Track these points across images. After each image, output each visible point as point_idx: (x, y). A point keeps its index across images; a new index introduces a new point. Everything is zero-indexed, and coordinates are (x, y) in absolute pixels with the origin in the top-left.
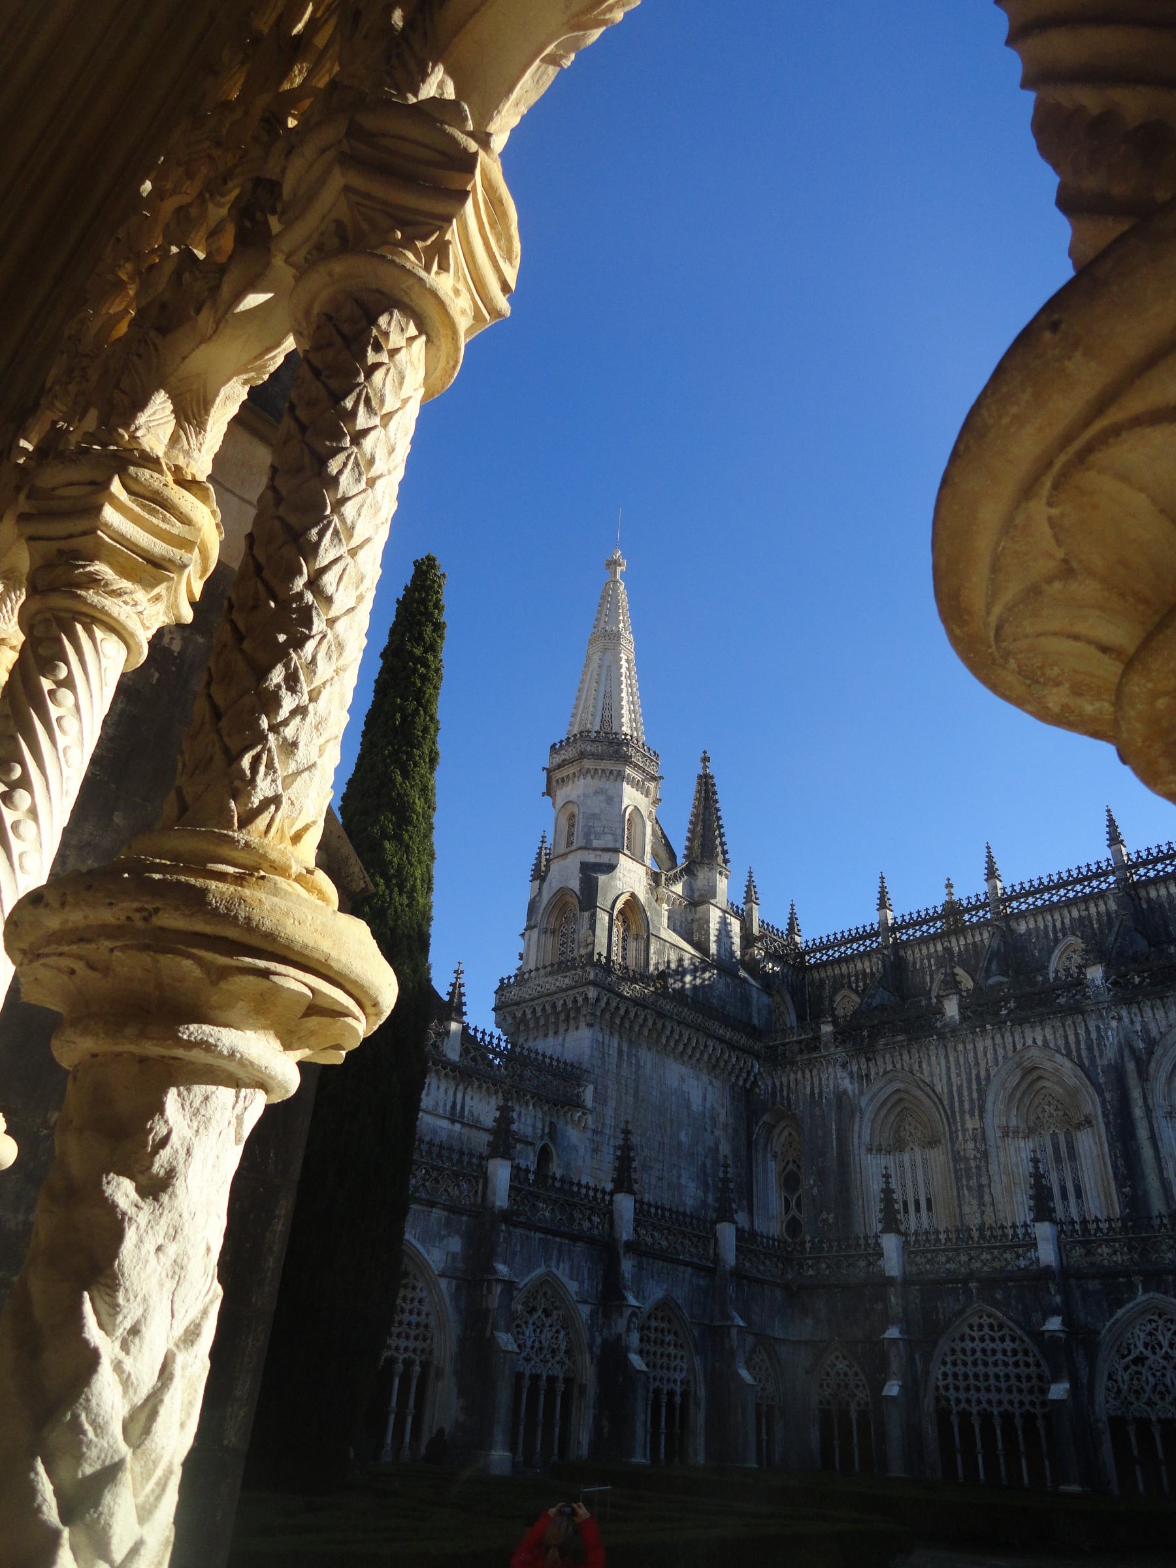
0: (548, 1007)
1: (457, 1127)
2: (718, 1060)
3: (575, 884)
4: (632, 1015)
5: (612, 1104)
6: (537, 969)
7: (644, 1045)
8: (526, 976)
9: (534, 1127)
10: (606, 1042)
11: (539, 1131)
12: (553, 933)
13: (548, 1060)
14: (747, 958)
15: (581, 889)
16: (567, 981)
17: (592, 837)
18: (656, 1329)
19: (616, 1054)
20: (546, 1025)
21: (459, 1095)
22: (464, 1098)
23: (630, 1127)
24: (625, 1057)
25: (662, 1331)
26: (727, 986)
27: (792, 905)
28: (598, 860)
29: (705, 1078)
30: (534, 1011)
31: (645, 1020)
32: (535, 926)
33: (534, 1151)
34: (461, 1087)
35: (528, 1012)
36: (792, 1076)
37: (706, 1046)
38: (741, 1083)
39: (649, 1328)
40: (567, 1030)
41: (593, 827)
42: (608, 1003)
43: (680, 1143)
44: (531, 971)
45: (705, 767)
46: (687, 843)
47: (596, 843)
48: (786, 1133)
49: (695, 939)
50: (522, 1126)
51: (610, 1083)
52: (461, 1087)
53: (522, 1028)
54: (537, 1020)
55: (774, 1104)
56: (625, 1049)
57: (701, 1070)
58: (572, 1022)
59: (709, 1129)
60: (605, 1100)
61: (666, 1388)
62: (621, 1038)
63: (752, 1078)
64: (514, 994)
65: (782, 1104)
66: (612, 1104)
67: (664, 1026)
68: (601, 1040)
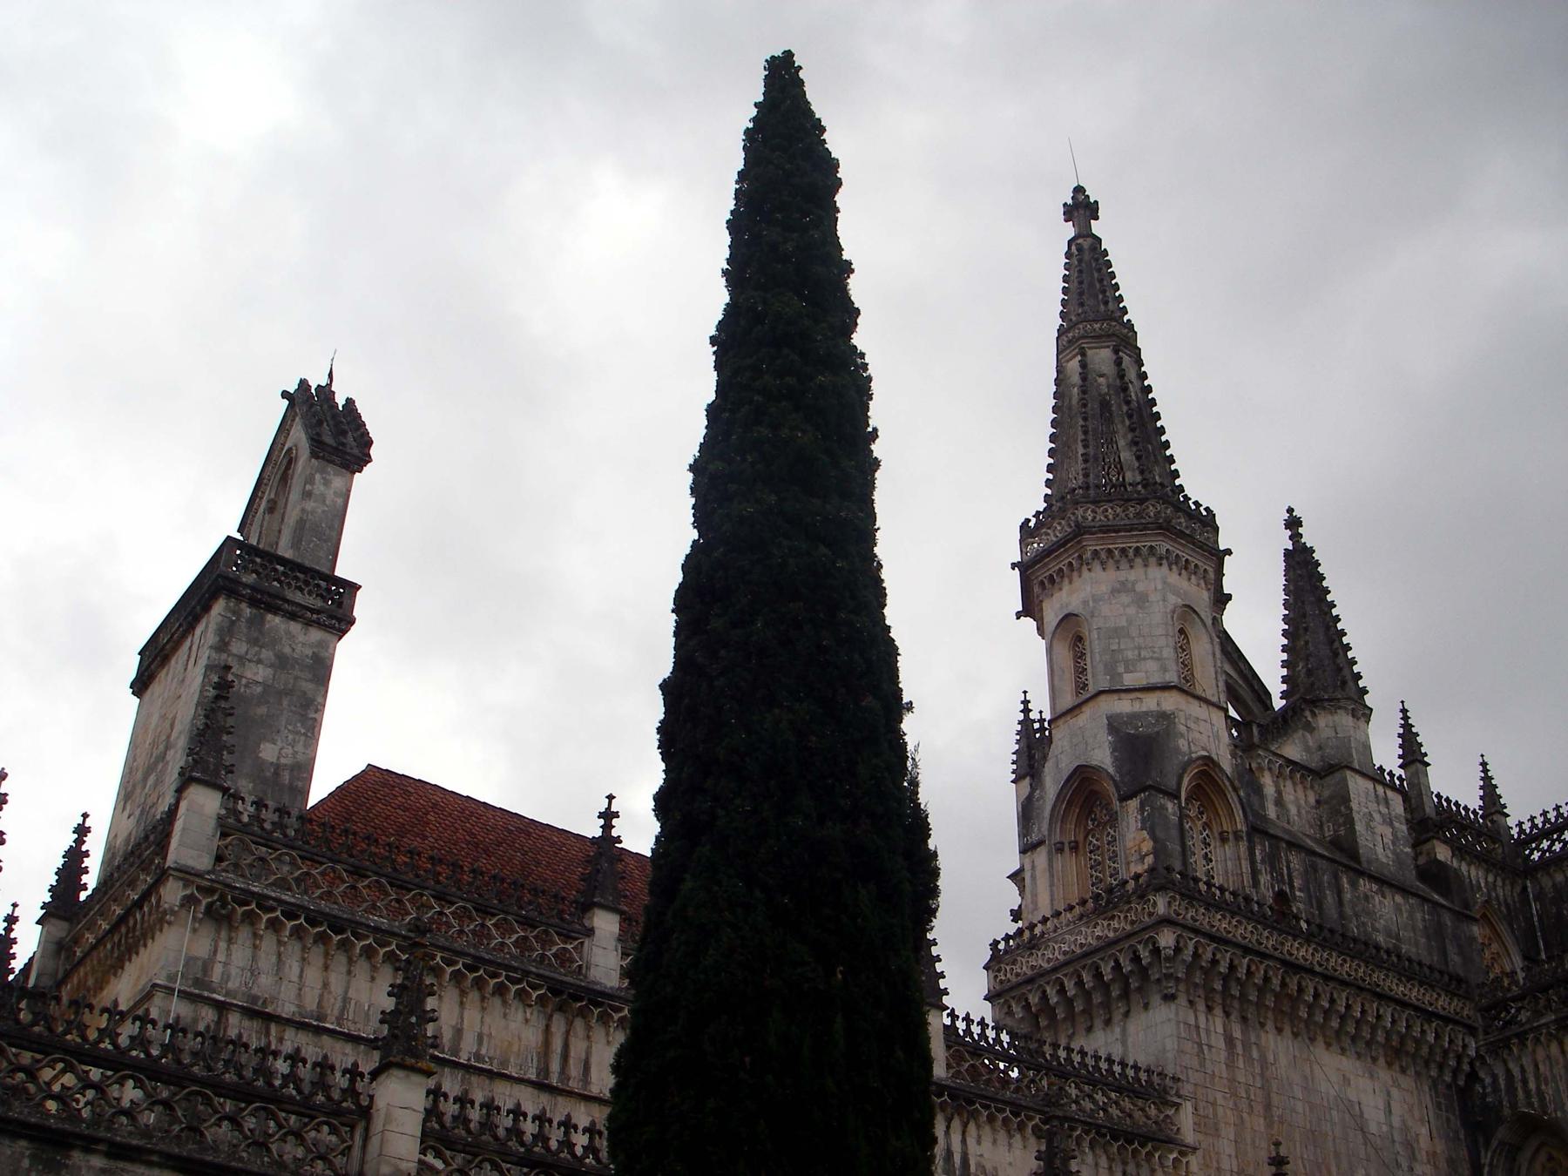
0: (1086, 977)
2: (1402, 1038)
3: (1102, 756)
4: (1242, 973)
6: (1057, 914)
7: (1270, 1025)
8: (1037, 931)
10: (1202, 1025)
12: (1075, 848)
13: (1104, 1066)
14: (1422, 860)
15: (1116, 759)
16: (1115, 924)
17: (1121, 669)
19: (1222, 1044)
20: (1087, 1012)
21: (956, 1139)
22: (964, 1141)
23: (1283, 1152)
24: (1239, 1049)
26: (1398, 908)
27: (1484, 764)
28: (1138, 707)
29: (1384, 1075)
30: (1062, 991)
31: (1266, 979)
32: (1040, 843)
34: (956, 1124)
35: (1051, 992)
36: (1541, 1054)
37: (1379, 1017)
38: (1448, 1078)
40: (1127, 1014)
41: (1120, 651)
42: (1196, 955)
44: (1045, 920)
45: (1296, 537)
46: (1284, 672)
47: (1129, 680)
48: (1542, 1157)
49: (1329, 833)
51: (1219, 1096)
52: (956, 1124)
53: (1043, 1022)
54: (1069, 1002)
55: (1514, 1106)
56: (1237, 1034)
57: (1374, 1060)
58: (1135, 997)
59: (1405, 1165)
62: (1227, 1014)
63: (1466, 1067)
64: (1025, 966)
65: (1530, 1105)
66: (1228, 1132)
67: (1301, 990)
68: (1192, 1022)
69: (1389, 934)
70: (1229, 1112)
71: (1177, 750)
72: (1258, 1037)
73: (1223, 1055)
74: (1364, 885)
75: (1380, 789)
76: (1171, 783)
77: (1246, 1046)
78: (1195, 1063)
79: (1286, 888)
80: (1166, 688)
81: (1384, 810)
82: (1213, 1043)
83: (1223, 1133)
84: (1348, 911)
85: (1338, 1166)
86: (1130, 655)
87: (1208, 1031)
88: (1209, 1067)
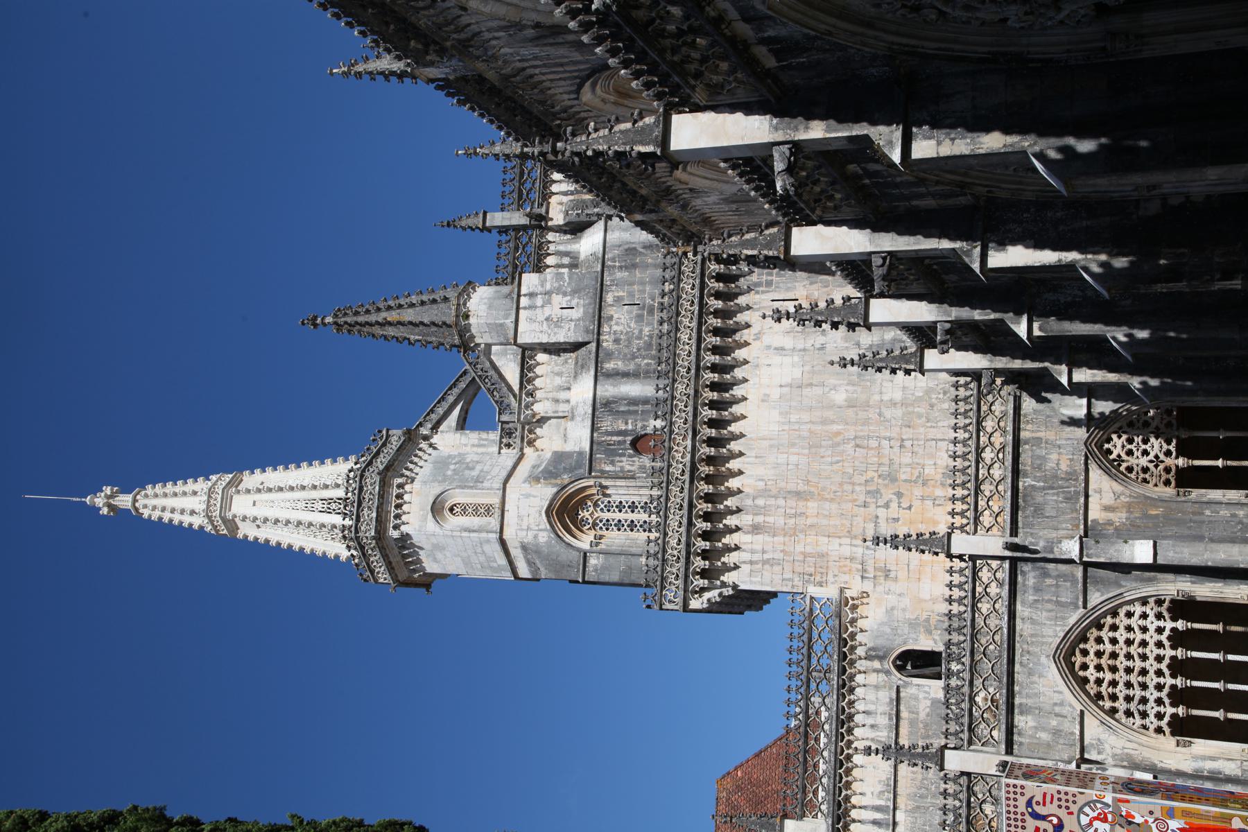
1: (900, 816)
5: (824, 544)
9: (877, 687)
11: (882, 677)
17: (495, 565)
18: (1099, 668)
19: (759, 538)
24: (760, 519)
25: (1099, 654)
33: (906, 684)
39: (1099, 682)
43: (851, 404)
47: (502, 561)
50: (881, 709)
51: (800, 548)
60: (822, 556)
61: (1168, 653)
66: (824, 544)
69: (639, 318)
70: (809, 539)
71: (548, 543)
72: (748, 495)
73: (768, 539)
74: (607, 344)
75: (524, 301)
76: (575, 557)
77: (757, 511)
78: (777, 569)
79: (629, 438)
80: (503, 543)
81: (539, 301)
82: (758, 547)
83: (824, 549)
84: (631, 367)
85: (833, 422)
86: (482, 558)
87: (753, 552)
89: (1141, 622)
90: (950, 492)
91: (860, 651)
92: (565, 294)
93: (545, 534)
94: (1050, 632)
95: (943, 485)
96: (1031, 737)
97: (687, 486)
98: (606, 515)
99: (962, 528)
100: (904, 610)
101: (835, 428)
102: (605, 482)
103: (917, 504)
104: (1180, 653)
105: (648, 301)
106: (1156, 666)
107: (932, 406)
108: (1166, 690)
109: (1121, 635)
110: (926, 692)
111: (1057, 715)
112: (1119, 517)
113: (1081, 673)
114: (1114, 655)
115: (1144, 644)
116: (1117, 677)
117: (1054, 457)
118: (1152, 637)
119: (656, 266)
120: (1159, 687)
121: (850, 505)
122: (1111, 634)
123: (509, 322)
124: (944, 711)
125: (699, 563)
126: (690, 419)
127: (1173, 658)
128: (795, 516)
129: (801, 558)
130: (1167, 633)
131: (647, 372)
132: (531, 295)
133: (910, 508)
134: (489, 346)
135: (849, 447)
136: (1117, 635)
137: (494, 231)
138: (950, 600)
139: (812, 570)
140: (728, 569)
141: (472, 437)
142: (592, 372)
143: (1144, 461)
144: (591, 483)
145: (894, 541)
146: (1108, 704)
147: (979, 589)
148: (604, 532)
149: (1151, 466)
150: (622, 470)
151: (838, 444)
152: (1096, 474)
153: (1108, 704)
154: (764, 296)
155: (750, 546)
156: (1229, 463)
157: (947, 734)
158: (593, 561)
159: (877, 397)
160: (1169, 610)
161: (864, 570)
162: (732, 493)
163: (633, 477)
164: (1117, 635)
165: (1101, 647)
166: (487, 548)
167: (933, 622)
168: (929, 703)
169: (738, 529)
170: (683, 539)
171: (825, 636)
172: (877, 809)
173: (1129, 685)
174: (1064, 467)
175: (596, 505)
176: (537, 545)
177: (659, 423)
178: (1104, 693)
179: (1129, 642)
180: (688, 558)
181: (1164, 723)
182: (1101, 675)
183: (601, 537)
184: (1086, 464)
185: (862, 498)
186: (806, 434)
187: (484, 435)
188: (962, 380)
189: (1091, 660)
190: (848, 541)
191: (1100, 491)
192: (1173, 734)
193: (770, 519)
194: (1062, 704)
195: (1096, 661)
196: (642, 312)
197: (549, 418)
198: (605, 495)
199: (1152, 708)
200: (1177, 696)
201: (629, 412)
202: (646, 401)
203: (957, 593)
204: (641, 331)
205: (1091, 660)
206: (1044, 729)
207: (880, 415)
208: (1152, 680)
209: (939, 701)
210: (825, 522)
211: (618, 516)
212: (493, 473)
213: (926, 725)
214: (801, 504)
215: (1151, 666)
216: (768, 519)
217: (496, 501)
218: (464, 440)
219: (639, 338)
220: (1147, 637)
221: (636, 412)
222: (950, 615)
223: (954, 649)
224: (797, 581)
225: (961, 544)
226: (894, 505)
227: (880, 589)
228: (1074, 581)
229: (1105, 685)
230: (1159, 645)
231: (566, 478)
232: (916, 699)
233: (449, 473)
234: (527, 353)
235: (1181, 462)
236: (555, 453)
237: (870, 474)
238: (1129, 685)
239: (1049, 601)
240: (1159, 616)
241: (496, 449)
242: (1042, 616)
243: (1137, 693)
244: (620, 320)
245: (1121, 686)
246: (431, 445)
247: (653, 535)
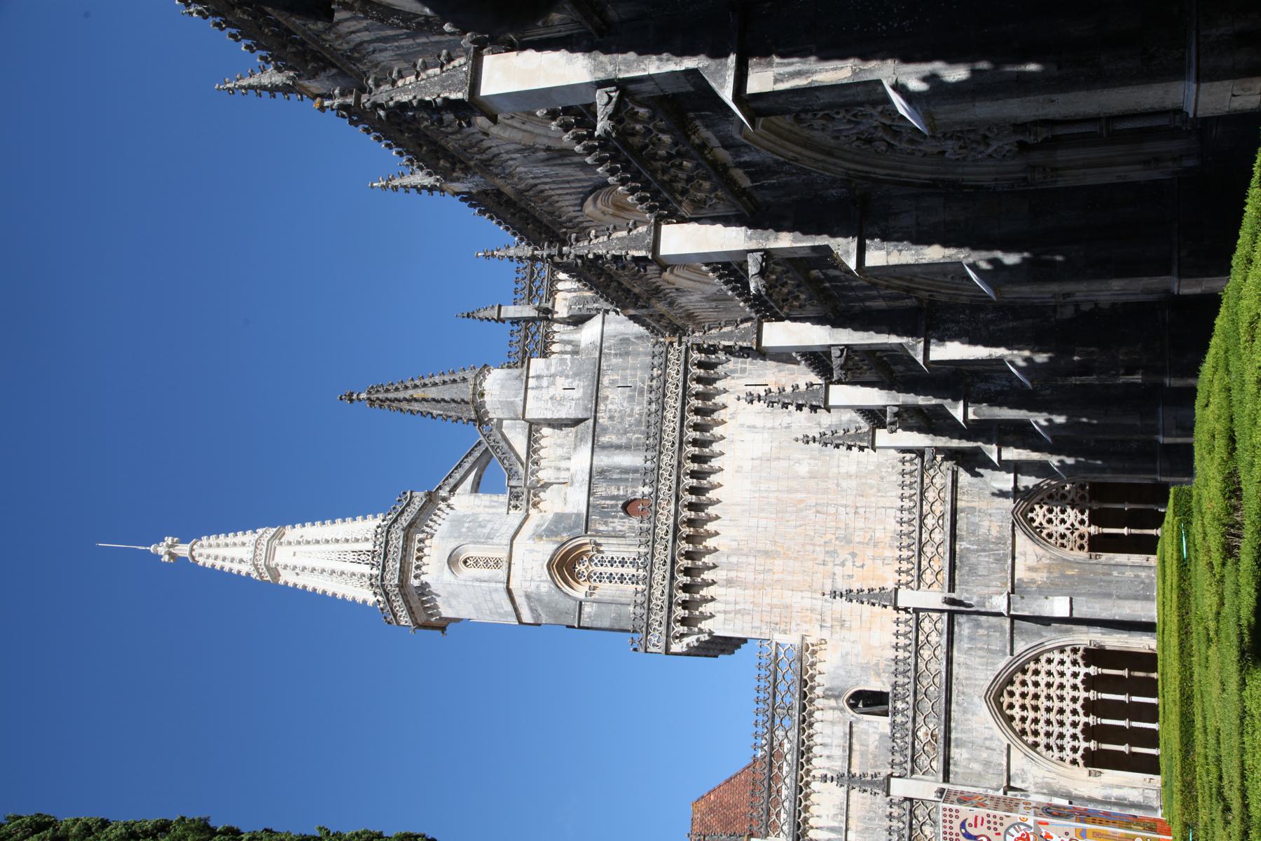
9: (833, 723)
11: (837, 713)
18: (1023, 707)
25: (1023, 695)
33: (858, 720)
39: (1023, 719)
43: (813, 476)
47: (509, 608)
50: (836, 742)
51: (767, 600)
61: (1082, 694)
69: (631, 398)
70: (775, 593)
72: (723, 554)
73: (740, 591)
74: (603, 420)
75: (532, 383)
76: (573, 605)
78: (747, 618)
79: (621, 503)
80: (509, 592)
81: (545, 382)
82: (732, 599)
84: (624, 441)
85: (797, 491)
86: (491, 605)
87: (726, 603)
88: (749, 607)
89: (1060, 668)
90: (898, 553)
91: (819, 691)
92: (567, 377)
93: (546, 585)
94: (982, 676)
95: (891, 547)
96: (965, 767)
97: (670, 544)
98: (599, 569)
99: (907, 584)
100: (857, 655)
101: (800, 496)
102: (599, 540)
103: (868, 563)
104: (1092, 695)
105: (639, 384)
106: (1072, 706)
107: (882, 478)
108: (1080, 727)
109: (1042, 679)
110: (875, 727)
111: (987, 748)
112: (1041, 577)
113: (1008, 712)
114: (1036, 697)
115: (1061, 686)
116: (1038, 715)
117: (986, 523)
118: (1068, 681)
119: (646, 354)
120: (1074, 725)
121: (811, 563)
122: (1034, 678)
123: (519, 400)
124: (890, 744)
125: (680, 612)
126: (674, 486)
127: (1086, 699)
128: (763, 572)
129: (768, 609)
130: (1081, 677)
131: (638, 445)
132: (538, 377)
133: (863, 566)
134: (500, 421)
135: (811, 514)
136: (1038, 678)
137: (508, 322)
138: (897, 648)
139: (777, 619)
140: (704, 617)
141: (484, 499)
142: (590, 445)
143: (1062, 529)
144: (587, 540)
145: (849, 595)
146: (1031, 739)
147: (921, 638)
148: (598, 584)
149: (1068, 533)
150: (614, 530)
151: (801, 510)
152: (1021, 538)
153: (1031, 739)
154: (738, 382)
155: (723, 598)
156: (1133, 531)
157: (892, 764)
158: (587, 609)
159: (835, 470)
160: (1083, 657)
161: (823, 620)
162: (709, 551)
163: (623, 537)
164: (1038, 678)
165: (1025, 689)
166: (495, 596)
167: (882, 666)
168: (877, 737)
169: (714, 583)
170: (666, 591)
171: (788, 677)
172: (832, 829)
173: (1048, 722)
174: (994, 532)
175: (591, 560)
176: (539, 594)
177: (647, 490)
178: (1028, 730)
179: (1049, 685)
180: (670, 608)
181: (1078, 756)
182: (1025, 714)
183: (595, 588)
184: (1013, 530)
185: (821, 557)
186: (773, 501)
187: (495, 498)
188: (908, 456)
189: (1017, 700)
190: (809, 594)
191: (1025, 554)
192: (1086, 765)
193: (742, 575)
194: (991, 739)
195: (1021, 701)
196: (634, 392)
197: (552, 484)
198: (599, 551)
199: (1068, 743)
200: (1090, 733)
201: (621, 480)
202: (636, 471)
203: (902, 641)
204: (632, 410)
205: (1017, 700)
206: (976, 760)
207: (837, 485)
208: (1068, 718)
209: (886, 735)
210: (789, 578)
211: (610, 570)
212: (502, 531)
213: (875, 756)
214: (769, 561)
215: (1068, 705)
216: (740, 574)
217: (503, 555)
218: (477, 501)
219: (631, 415)
220: (1064, 680)
221: (627, 480)
222: (896, 660)
223: (900, 689)
224: (765, 630)
225: (907, 598)
226: (849, 564)
227: (836, 636)
228: (1003, 631)
229: (1028, 722)
230: (1075, 687)
231: (565, 537)
232: (867, 733)
233: (464, 530)
234: (533, 427)
235: (1093, 530)
236: (556, 514)
237: (829, 536)
238: (1048, 722)
239: (981, 649)
240: (1075, 663)
241: (505, 510)
242: (975, 662)
243: (1056, 729)
244: (615, 400)
245: (1042, 723)
246: (448, 506)
247: (641, 587)
